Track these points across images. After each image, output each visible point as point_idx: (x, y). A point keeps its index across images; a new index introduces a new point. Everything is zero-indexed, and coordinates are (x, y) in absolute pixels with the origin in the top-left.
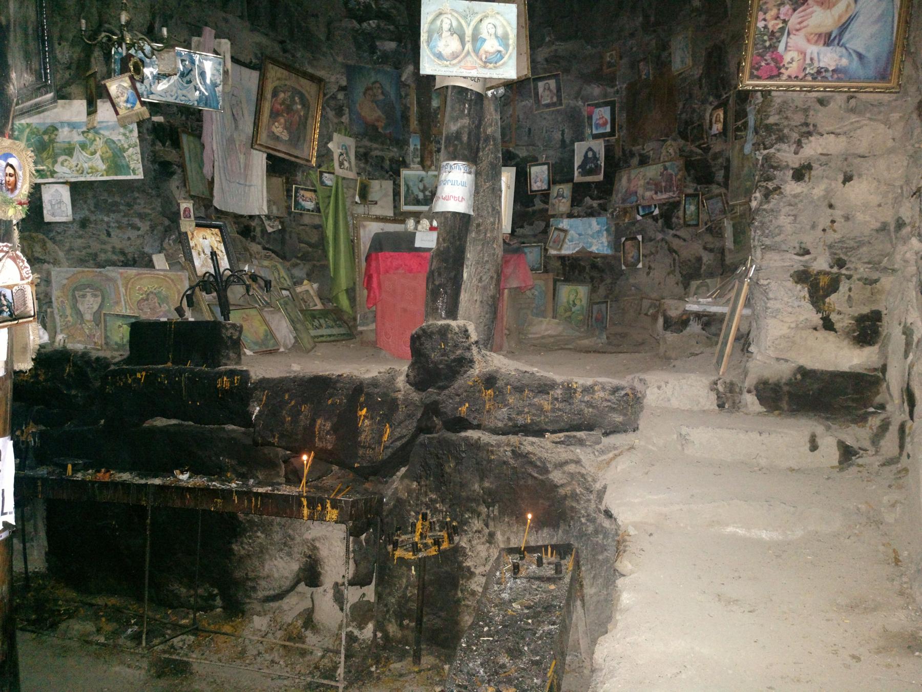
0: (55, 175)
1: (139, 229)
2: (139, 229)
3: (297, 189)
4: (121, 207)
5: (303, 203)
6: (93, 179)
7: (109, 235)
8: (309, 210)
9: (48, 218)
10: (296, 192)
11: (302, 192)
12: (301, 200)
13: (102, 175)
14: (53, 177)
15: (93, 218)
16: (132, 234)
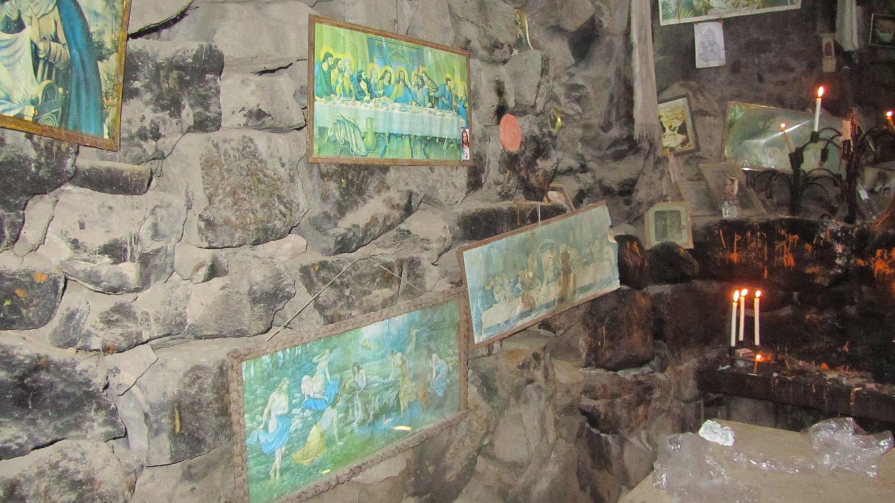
0: (709, 13)
1: (792, 70)
2: (792, 70)
3: (875, 17)
4: (773, 45)
5: (881, 35)
6: (748, 13)
7: (761, 79)
8: (886, 44)
9: (700, 64)
10: (875, 22)
11: (881, 22)
12: (878, 31)
13: (758, 8)
14: (706, 14)
15: (744, 60)
16: (790, 76)
